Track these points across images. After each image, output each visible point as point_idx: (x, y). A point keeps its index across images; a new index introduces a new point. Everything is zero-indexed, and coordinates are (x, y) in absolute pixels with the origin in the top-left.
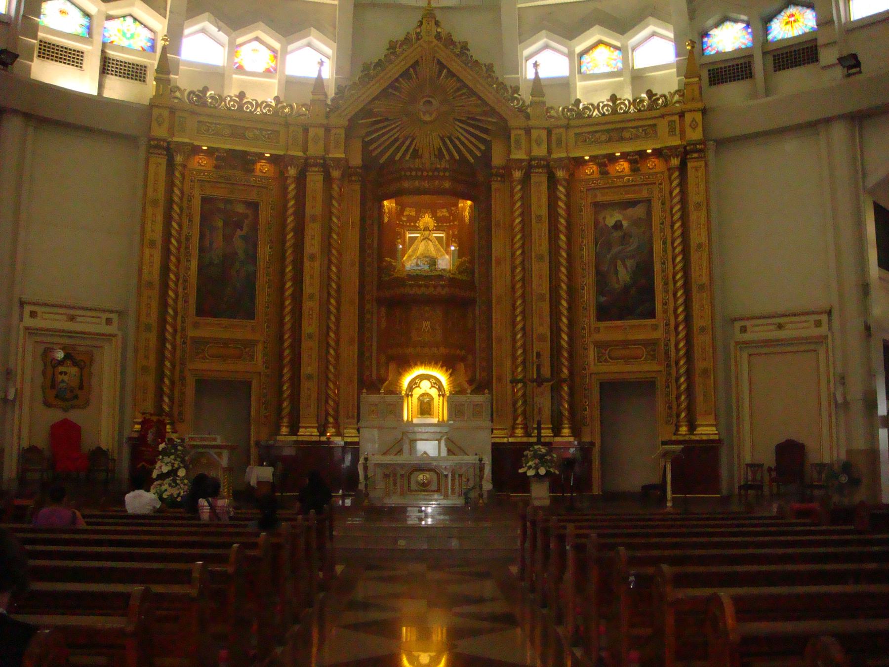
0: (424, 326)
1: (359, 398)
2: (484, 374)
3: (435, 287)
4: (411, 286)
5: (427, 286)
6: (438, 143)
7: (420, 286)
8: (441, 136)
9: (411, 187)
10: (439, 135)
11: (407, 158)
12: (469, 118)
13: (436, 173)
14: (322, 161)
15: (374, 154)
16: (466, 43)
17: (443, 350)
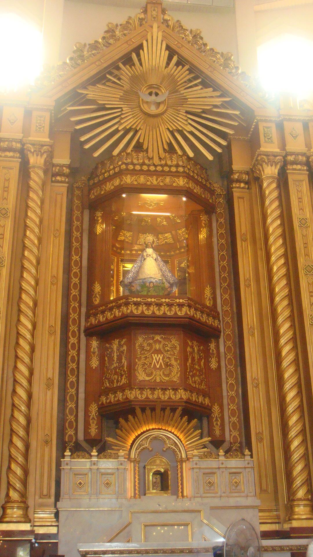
0: (154, 360)
1: (58, 464)
2: (235, 433)
3: (170, 305)
4: (137, 304)
5: (159, 305)
6: (167, 136)
7: (148, 304)
8: (171, 129)
9: (135, 183)
10: (168, 129)
11: (129, 150)
12: (204, 111)
13: (166, 169)
14: (19, 145)
15: (87, 147)
16: (200, 32)
17: (182, 395)
